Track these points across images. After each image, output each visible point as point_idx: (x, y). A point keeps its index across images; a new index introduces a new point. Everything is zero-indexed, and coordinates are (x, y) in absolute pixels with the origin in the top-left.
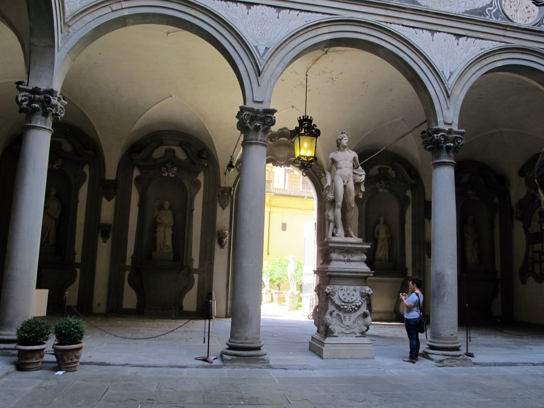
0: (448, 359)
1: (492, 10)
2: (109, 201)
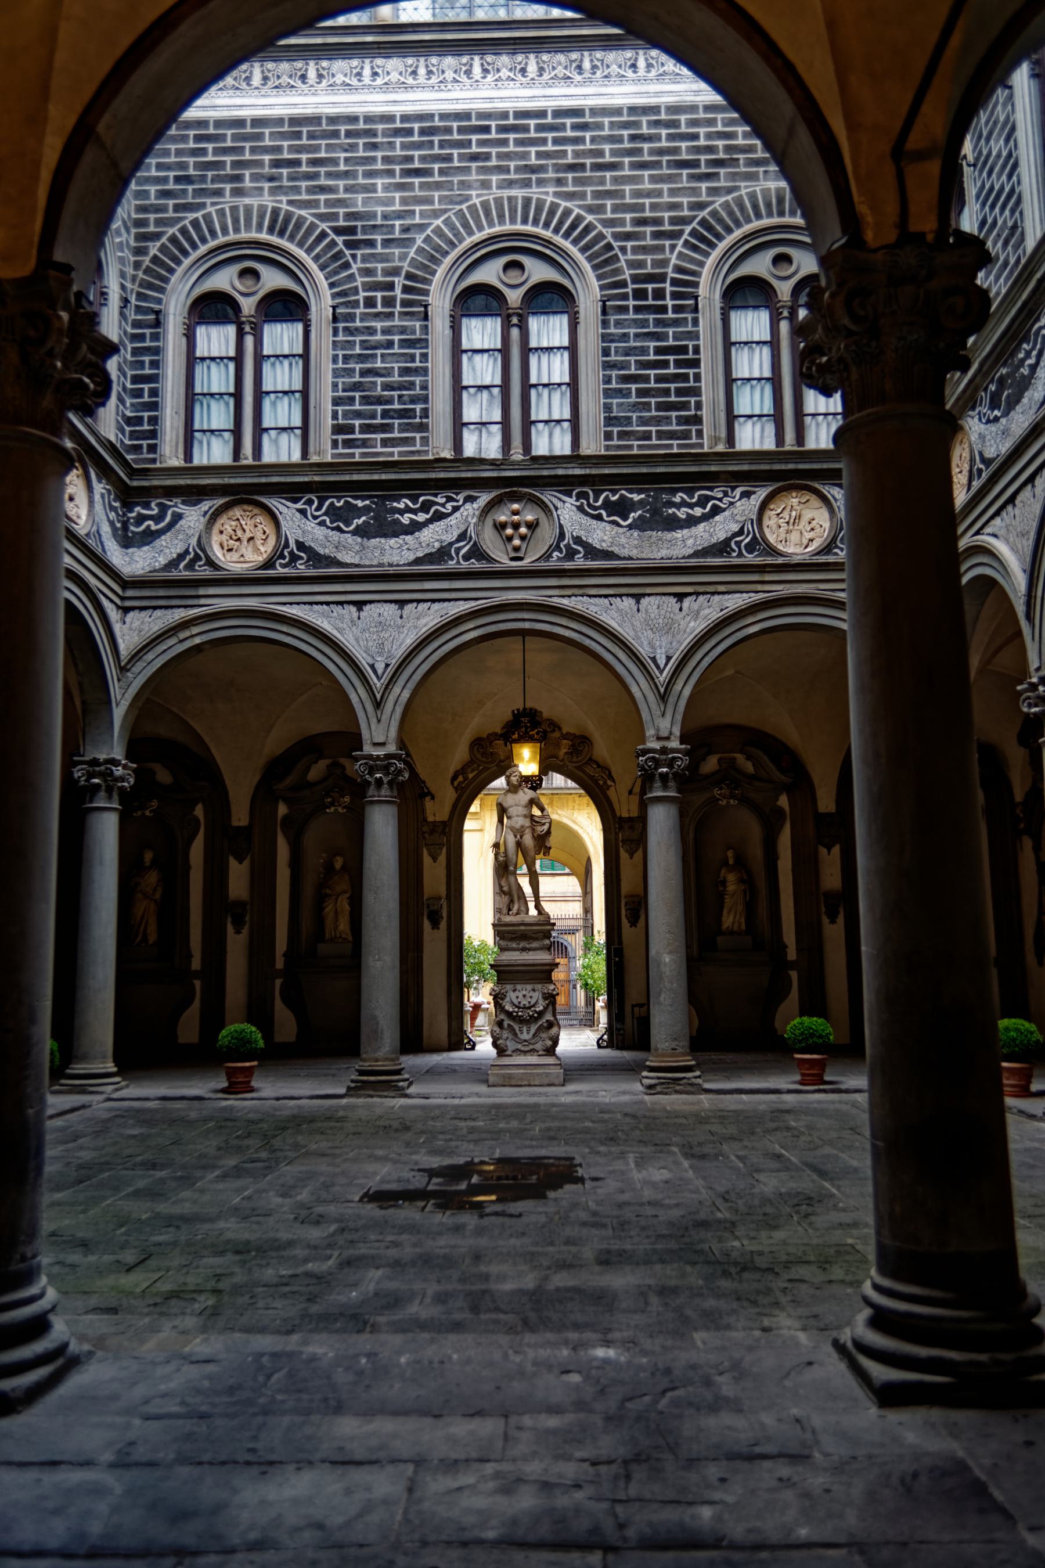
1: (742, 541)
2: (241, 862)
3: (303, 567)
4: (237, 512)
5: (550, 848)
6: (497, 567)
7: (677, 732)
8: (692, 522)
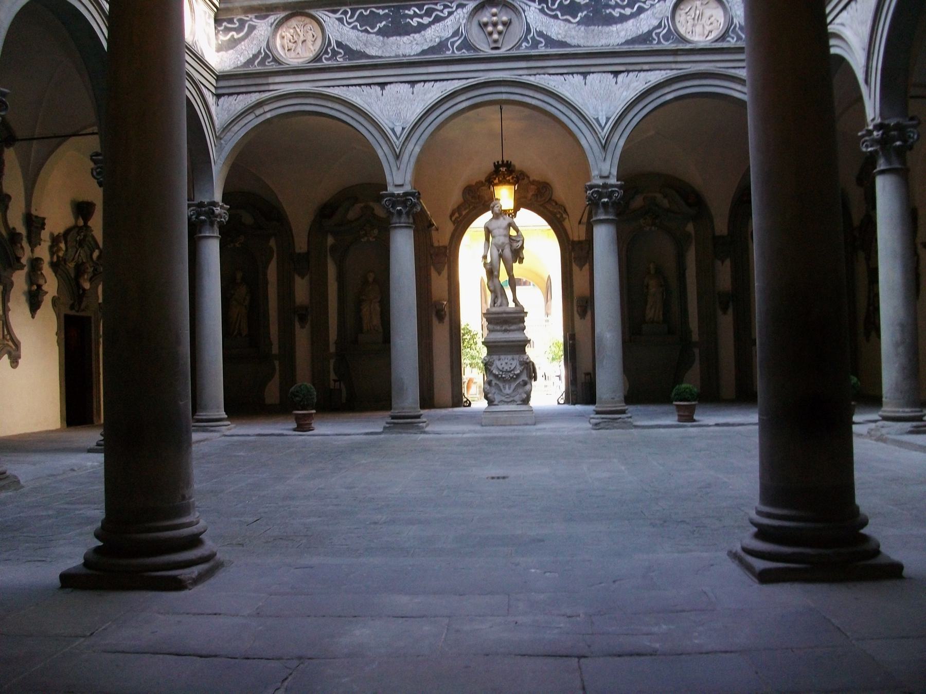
0: (605, 422)
1: (660, 33)
2: (303, 278)
3: (341, 60)
4: (294, 22)
5: (523, 258)
6: (481, 55)
7: (614, 172)
8: (623, 19)
